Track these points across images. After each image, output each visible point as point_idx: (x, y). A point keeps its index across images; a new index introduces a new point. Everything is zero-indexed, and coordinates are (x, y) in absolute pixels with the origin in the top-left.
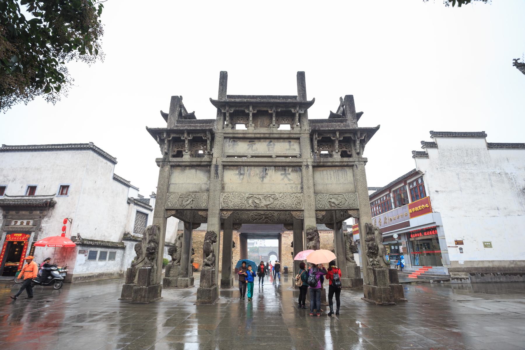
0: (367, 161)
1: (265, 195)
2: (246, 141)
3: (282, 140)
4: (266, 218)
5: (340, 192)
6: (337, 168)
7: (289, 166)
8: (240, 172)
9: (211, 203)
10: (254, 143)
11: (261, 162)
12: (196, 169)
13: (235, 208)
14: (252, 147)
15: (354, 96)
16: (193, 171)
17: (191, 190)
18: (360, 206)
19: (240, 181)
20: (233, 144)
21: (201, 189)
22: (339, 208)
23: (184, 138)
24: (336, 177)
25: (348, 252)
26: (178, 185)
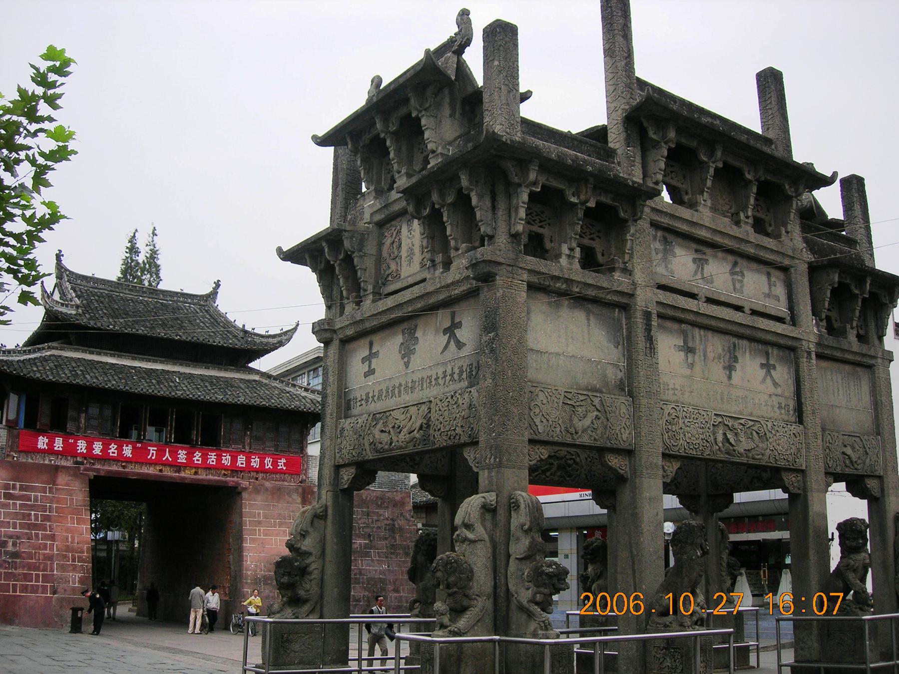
0: (893, 360)
1: (742, 421)
2: (688, 248)
3: (754, 265)
4: (560, 467)
5: (852, 429)
6: (847, 368)
7: (773, 344)
8: (685, 342)
9: (644, 430)
10: (704, 257)
11: (740, 324)
12: (588, 313)
13: (691, 451)
14: (702, 269)
15: (866, 182)
16: (580, 316)
17: (583, 381)
18: (885, 470)
19: (688, 372)
20: (665, 249)
21: (606, 383)
22: (855, 472)
23: (574, 200)
24: (846, 391)
25: (724, 574)
26: (545, 357)
